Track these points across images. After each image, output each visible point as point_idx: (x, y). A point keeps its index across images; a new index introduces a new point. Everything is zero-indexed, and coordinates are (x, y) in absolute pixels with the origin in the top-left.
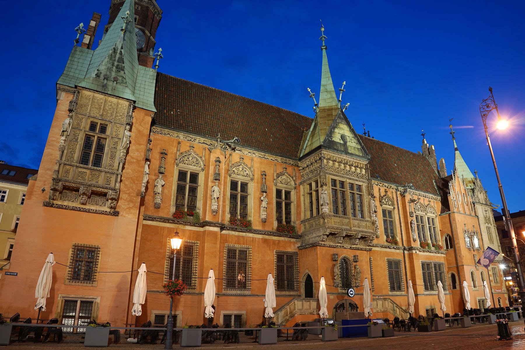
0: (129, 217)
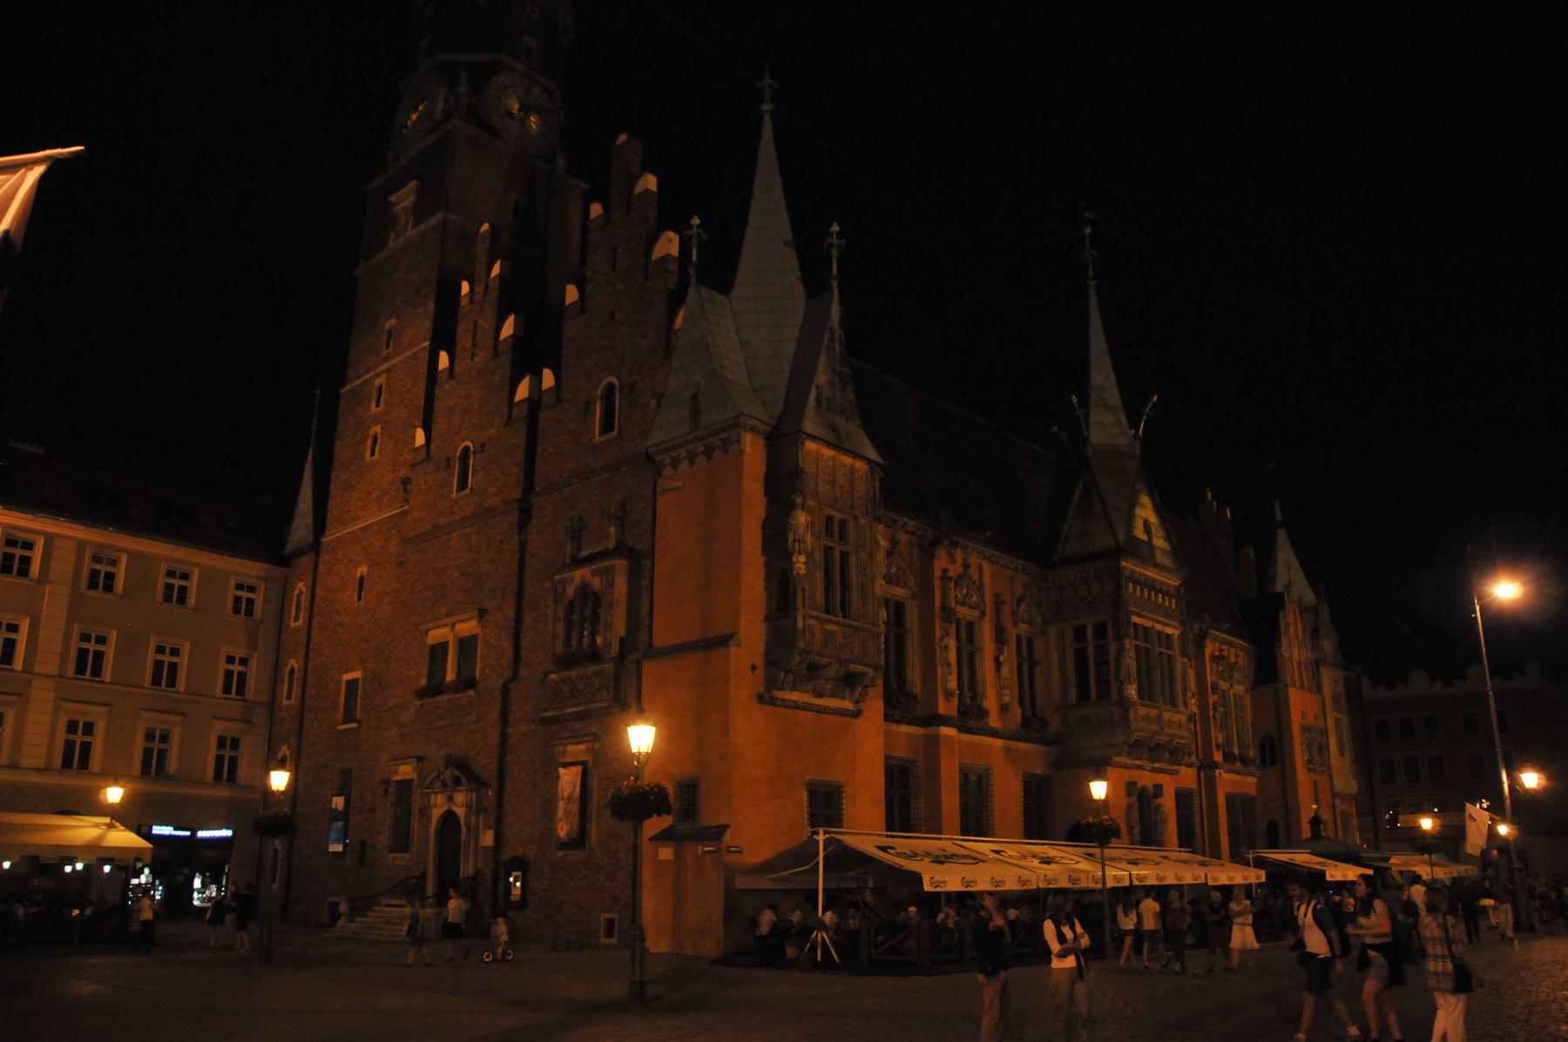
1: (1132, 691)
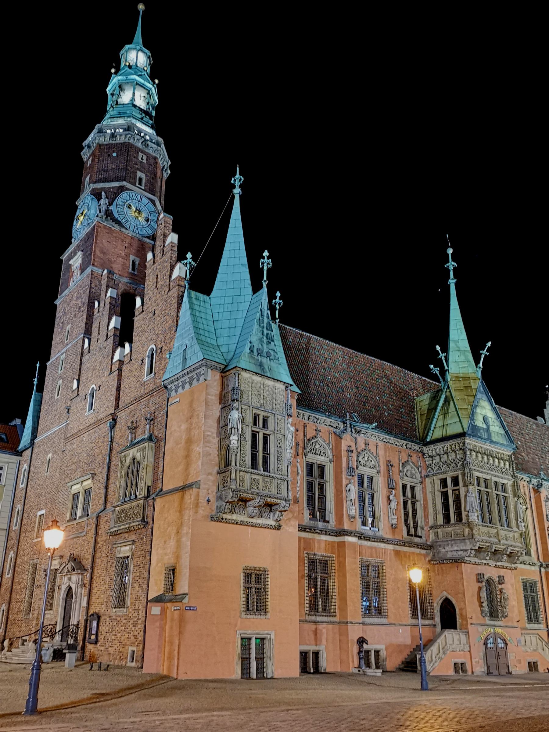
0: (290, 530)
1: (475, 517)
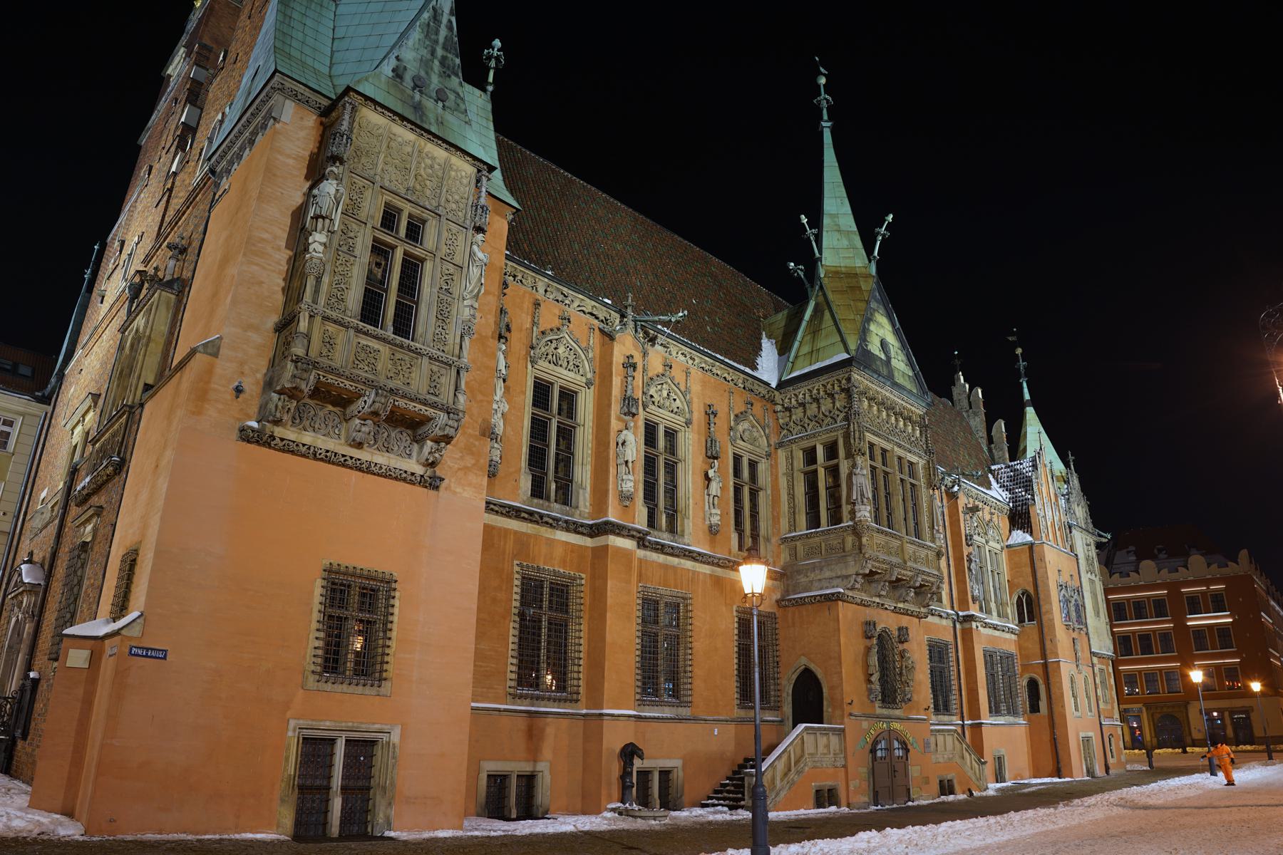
0: (465, 495)
